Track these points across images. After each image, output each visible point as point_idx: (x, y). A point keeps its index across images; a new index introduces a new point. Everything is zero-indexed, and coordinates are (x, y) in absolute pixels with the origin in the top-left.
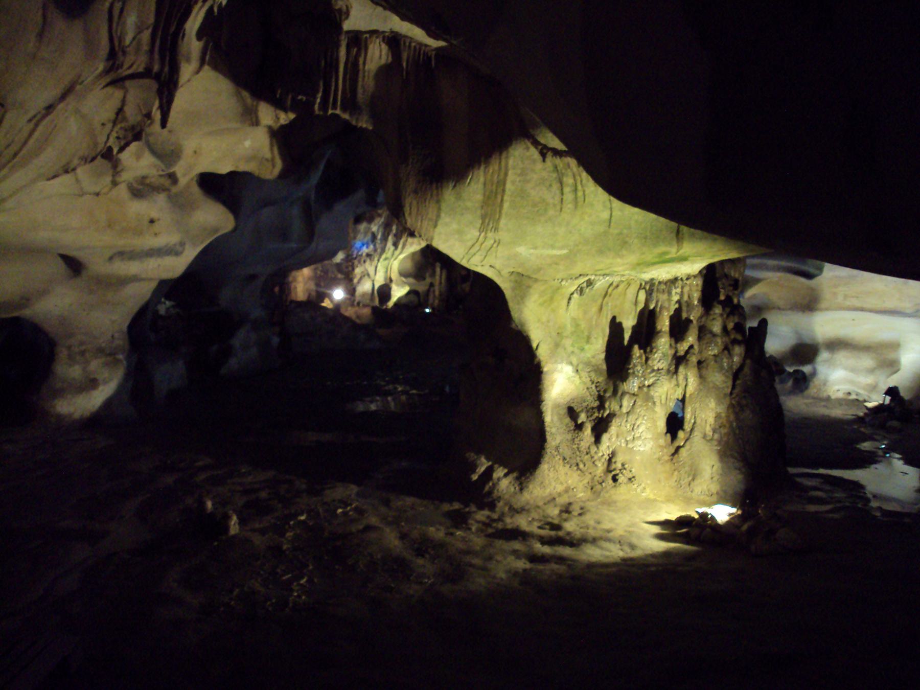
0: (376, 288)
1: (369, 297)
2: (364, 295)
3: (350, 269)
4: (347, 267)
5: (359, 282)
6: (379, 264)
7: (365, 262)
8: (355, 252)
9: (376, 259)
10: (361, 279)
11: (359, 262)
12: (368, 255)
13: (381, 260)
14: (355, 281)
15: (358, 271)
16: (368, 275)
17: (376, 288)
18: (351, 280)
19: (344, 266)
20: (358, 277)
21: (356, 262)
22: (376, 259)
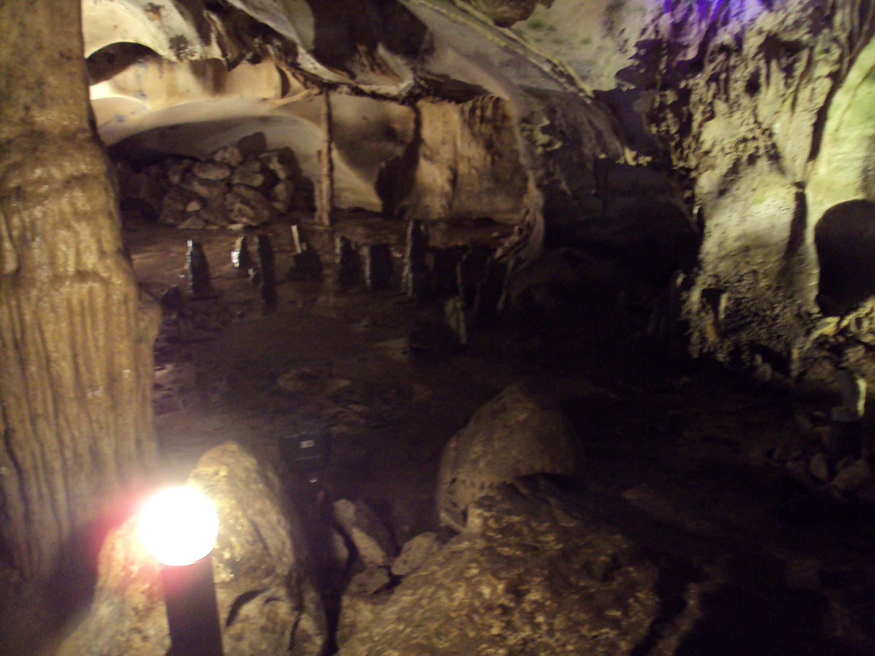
0: (814, 217)
1: (774, 262)
2: (749, 247)
3: (671, 125)
4: (656, 117)
5: (722, 192)
6: (841, 98)
7: (753, 87)
8: (693, 36)
9: (823, 70)
10: (735, 170)
11: (721, 83)
12: (776, 48)
13: (854, 76)
14: (706, 182)
15: (718, 133)
16: (775, 156)
17: (814, 217)
18: (687, 179)
19: (641, 106)
20: (724, 164)
21: (699, 85)
22: (823, 70)
